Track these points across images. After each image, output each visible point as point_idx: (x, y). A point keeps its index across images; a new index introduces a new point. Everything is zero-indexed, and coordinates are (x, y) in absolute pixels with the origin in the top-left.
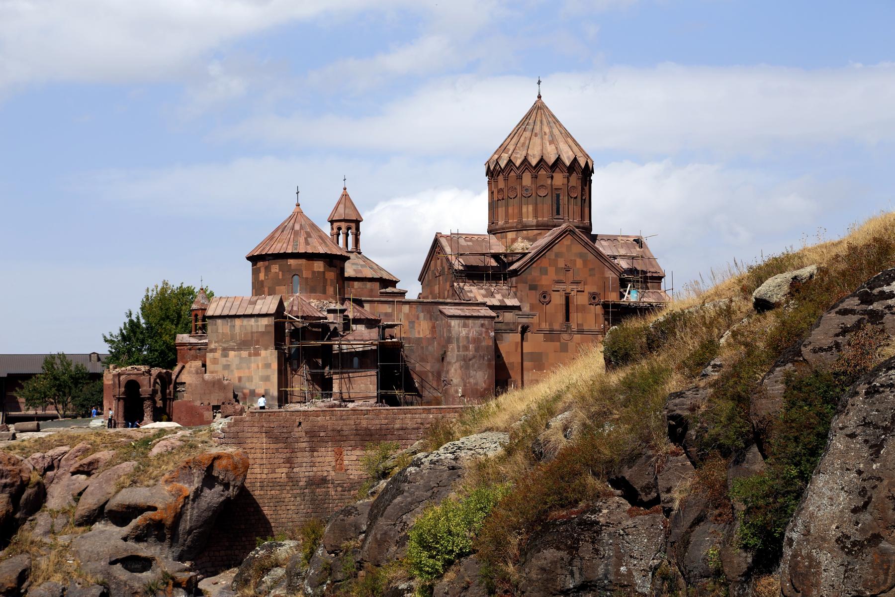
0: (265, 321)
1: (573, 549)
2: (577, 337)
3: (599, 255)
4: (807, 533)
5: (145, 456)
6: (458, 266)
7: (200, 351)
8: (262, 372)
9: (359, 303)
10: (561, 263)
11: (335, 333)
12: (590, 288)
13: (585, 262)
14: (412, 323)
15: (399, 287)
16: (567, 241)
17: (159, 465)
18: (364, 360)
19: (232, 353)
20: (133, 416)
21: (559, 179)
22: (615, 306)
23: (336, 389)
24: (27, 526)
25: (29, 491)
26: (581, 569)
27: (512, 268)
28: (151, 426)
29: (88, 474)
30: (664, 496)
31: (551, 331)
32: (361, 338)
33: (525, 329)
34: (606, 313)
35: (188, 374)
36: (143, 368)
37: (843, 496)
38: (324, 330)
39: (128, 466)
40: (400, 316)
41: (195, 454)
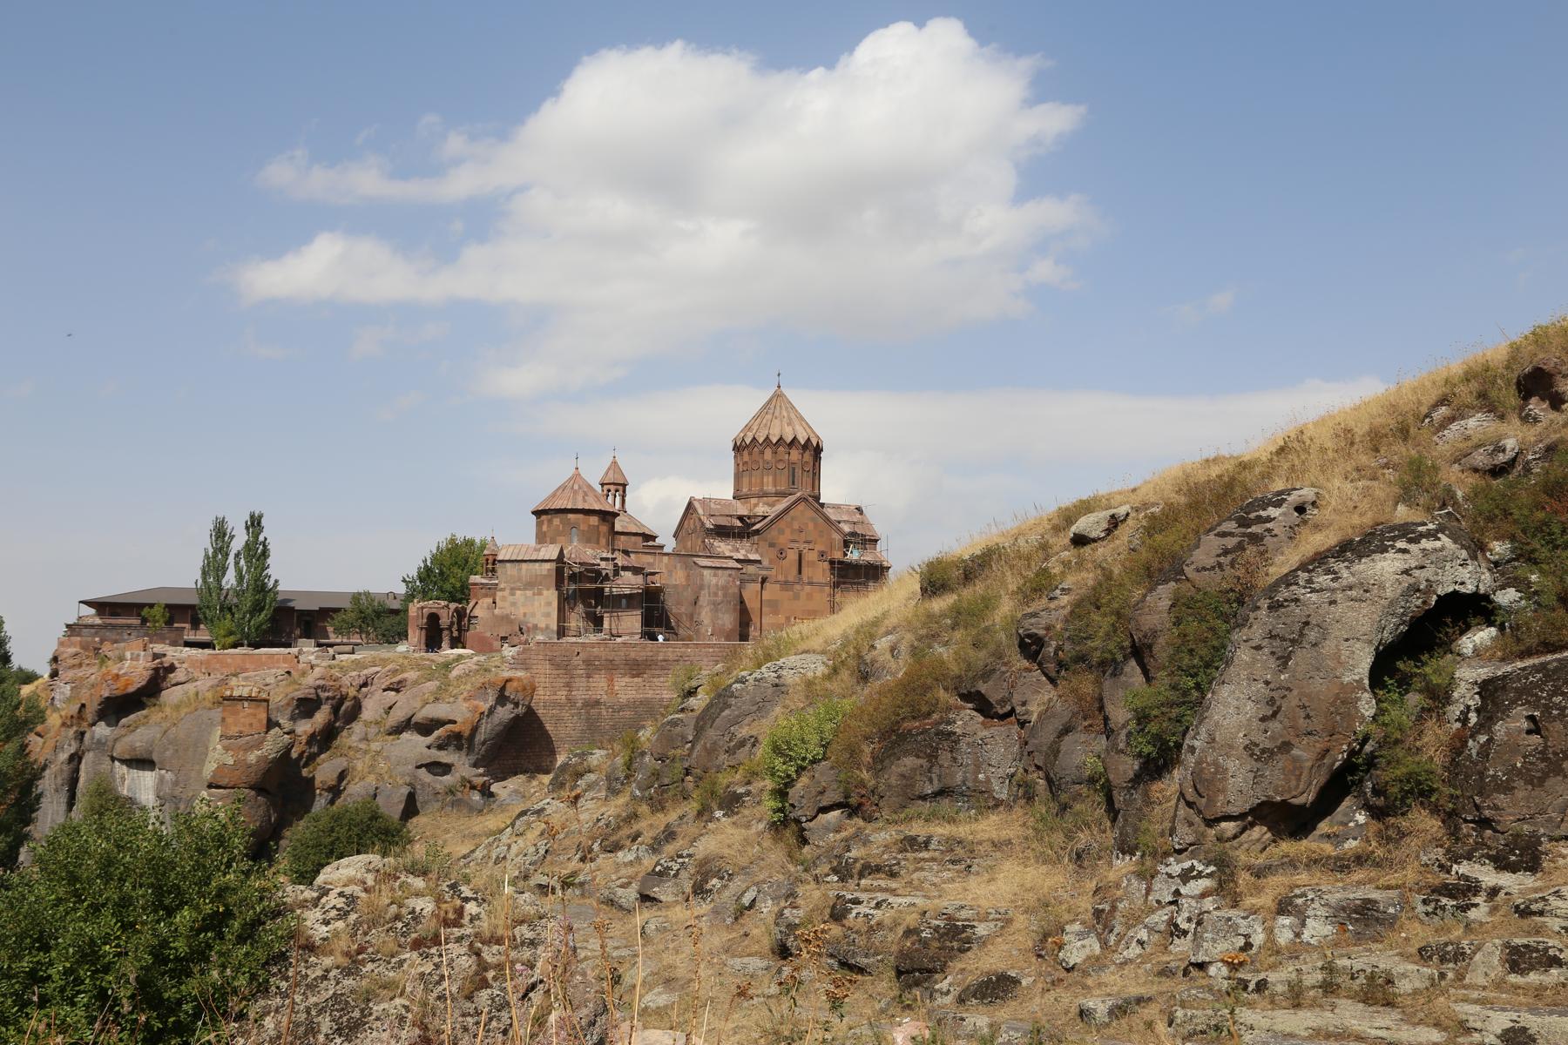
0: (547, 566)
1: (932, 757)
2: (808, 588)
3: (827, 519)
4: (1212, 740)
5: (446, 677)
6: (708, 525)
7: (491, 590)
9: (626, 553)
10: (796, 526)
11: (607, 578)
12: (819, 547)
13: (816, 525)
14: (670, 572)
15: (658, 541)
16: (802, 506)
17: (459, 686)
18: (631, 601)
20: (433, 643)
21: (795, 455)
22: (840, 562)
23: (606, 625)
24: (345, 733)
25: (347, 704)
26: (939, 776)
27: (757, 527)
28: (448, 652)
29: (398, 691)
30: (1019, 709)
31: (786, 582)
32: (628, 583)
33: (764, 580)
34: (832, 568)
35: (480, 609)
36: (443, 603)
37: (1250, 706)
38: (597, 575)
39: (432, 685)
40: (659, 565)
41: (489, 676)
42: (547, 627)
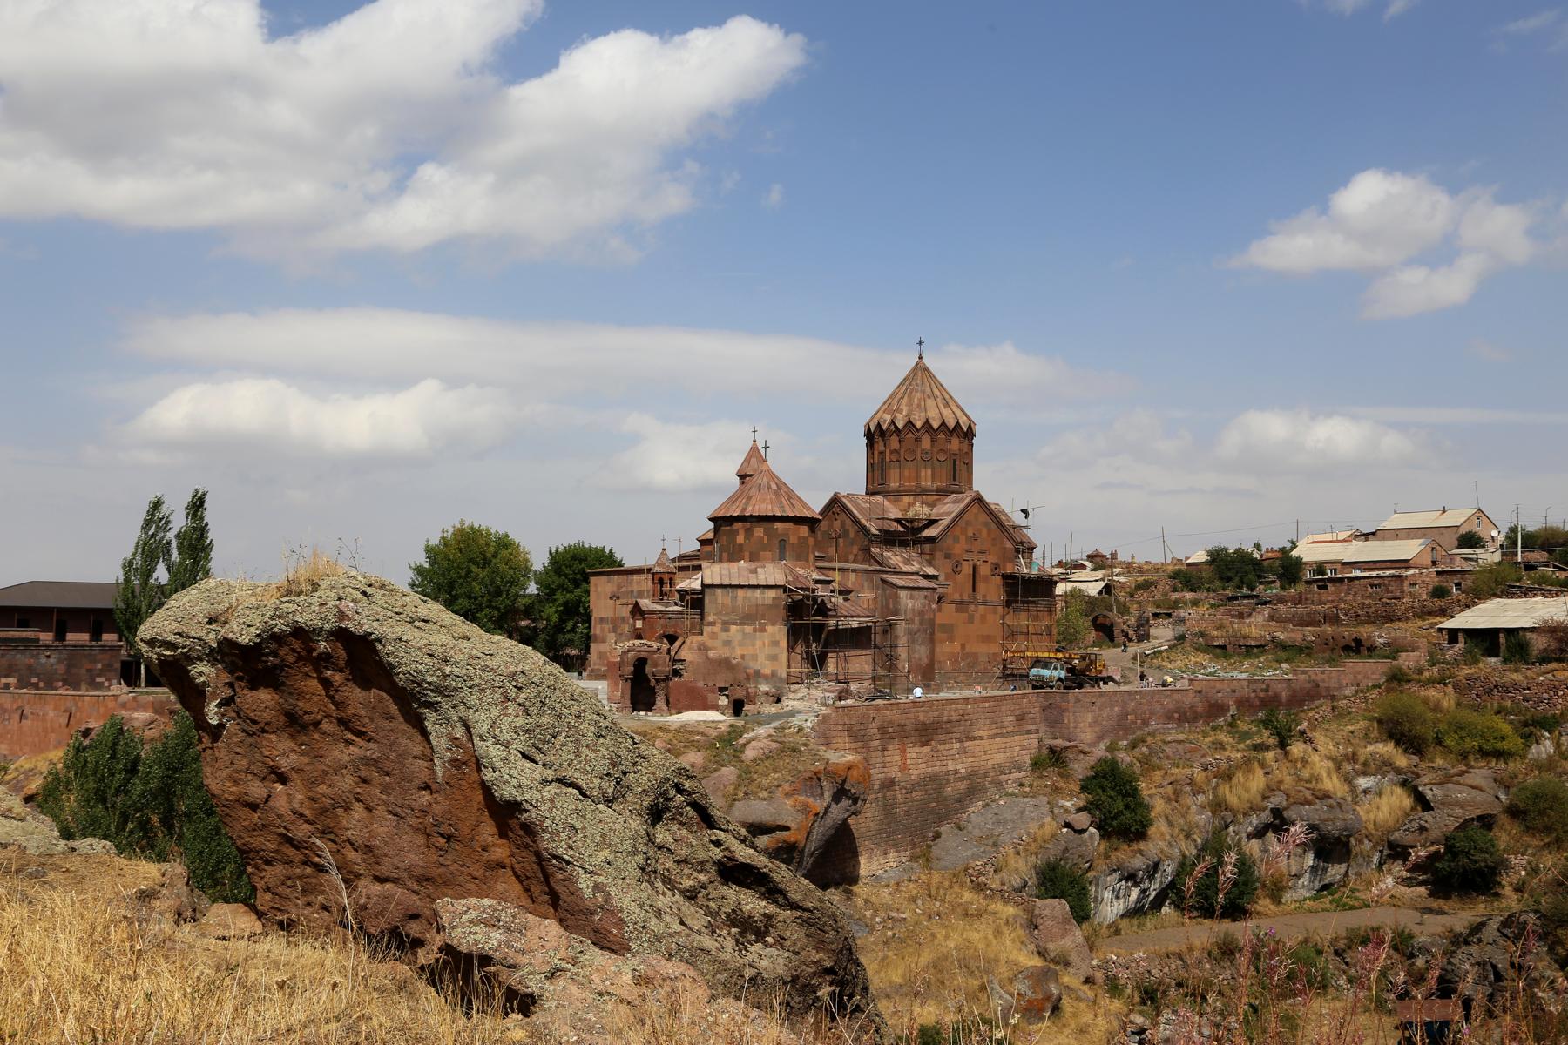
0: (772, 593)
8: (768, 650)
19: (733, 628)
42: (774, 674)
